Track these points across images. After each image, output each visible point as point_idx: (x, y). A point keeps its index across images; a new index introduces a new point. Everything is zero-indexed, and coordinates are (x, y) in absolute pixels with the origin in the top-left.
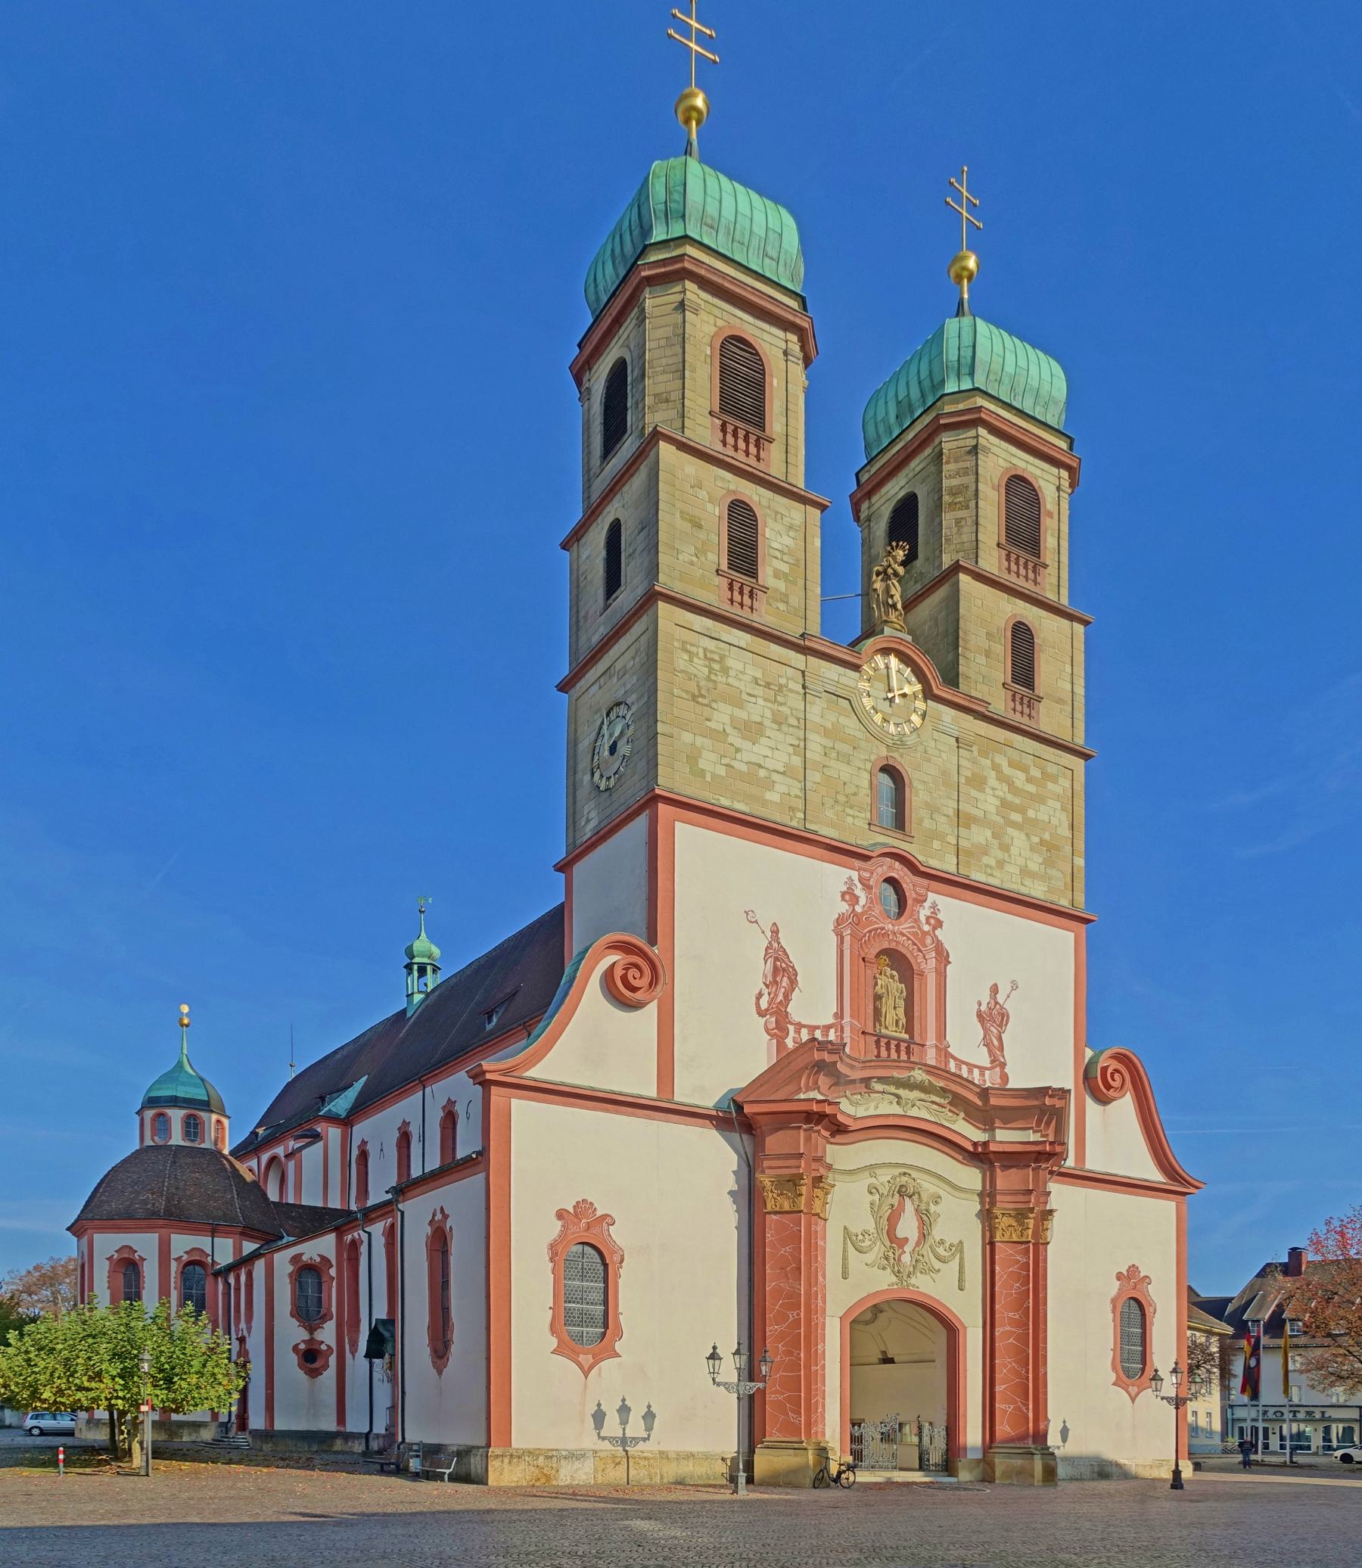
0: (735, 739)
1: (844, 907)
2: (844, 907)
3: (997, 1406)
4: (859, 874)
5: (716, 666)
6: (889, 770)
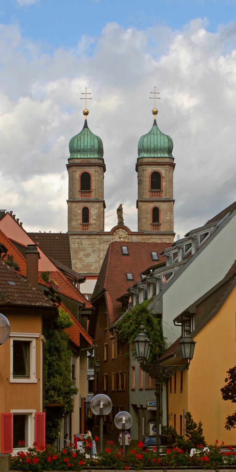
0: (84, 259)
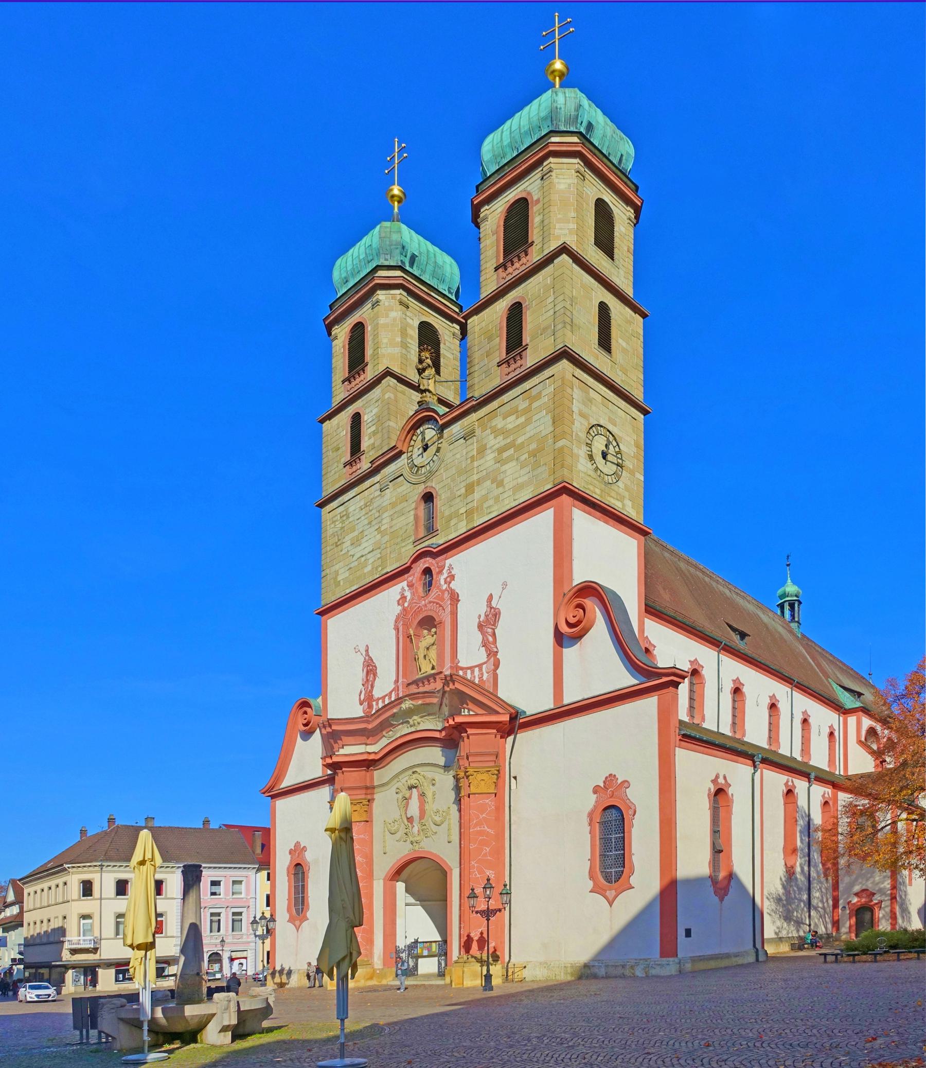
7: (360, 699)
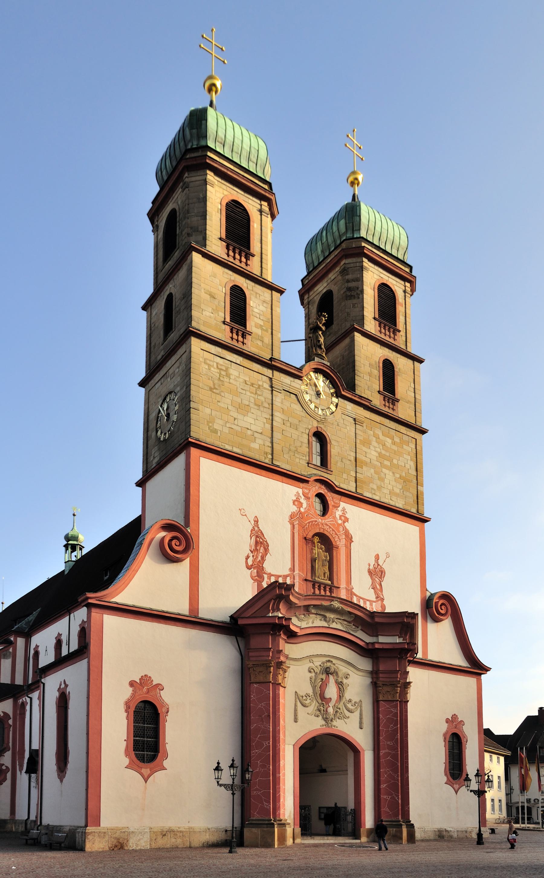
1: (294, 509)
2: (294, 509)
3: (382, 796)
4: (303, 491)
5: (223, 373)
6: (320, 436)
7: (247, 562)
